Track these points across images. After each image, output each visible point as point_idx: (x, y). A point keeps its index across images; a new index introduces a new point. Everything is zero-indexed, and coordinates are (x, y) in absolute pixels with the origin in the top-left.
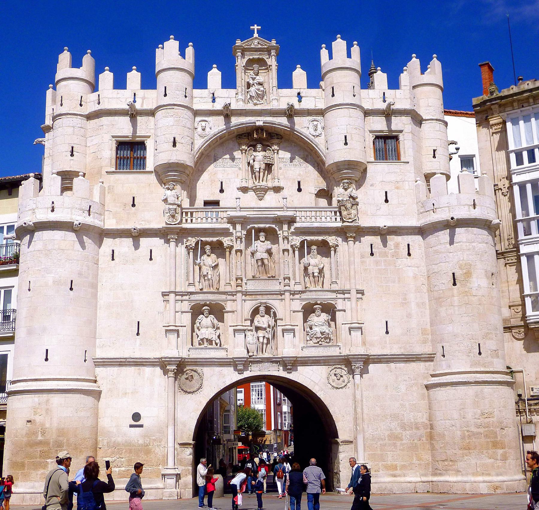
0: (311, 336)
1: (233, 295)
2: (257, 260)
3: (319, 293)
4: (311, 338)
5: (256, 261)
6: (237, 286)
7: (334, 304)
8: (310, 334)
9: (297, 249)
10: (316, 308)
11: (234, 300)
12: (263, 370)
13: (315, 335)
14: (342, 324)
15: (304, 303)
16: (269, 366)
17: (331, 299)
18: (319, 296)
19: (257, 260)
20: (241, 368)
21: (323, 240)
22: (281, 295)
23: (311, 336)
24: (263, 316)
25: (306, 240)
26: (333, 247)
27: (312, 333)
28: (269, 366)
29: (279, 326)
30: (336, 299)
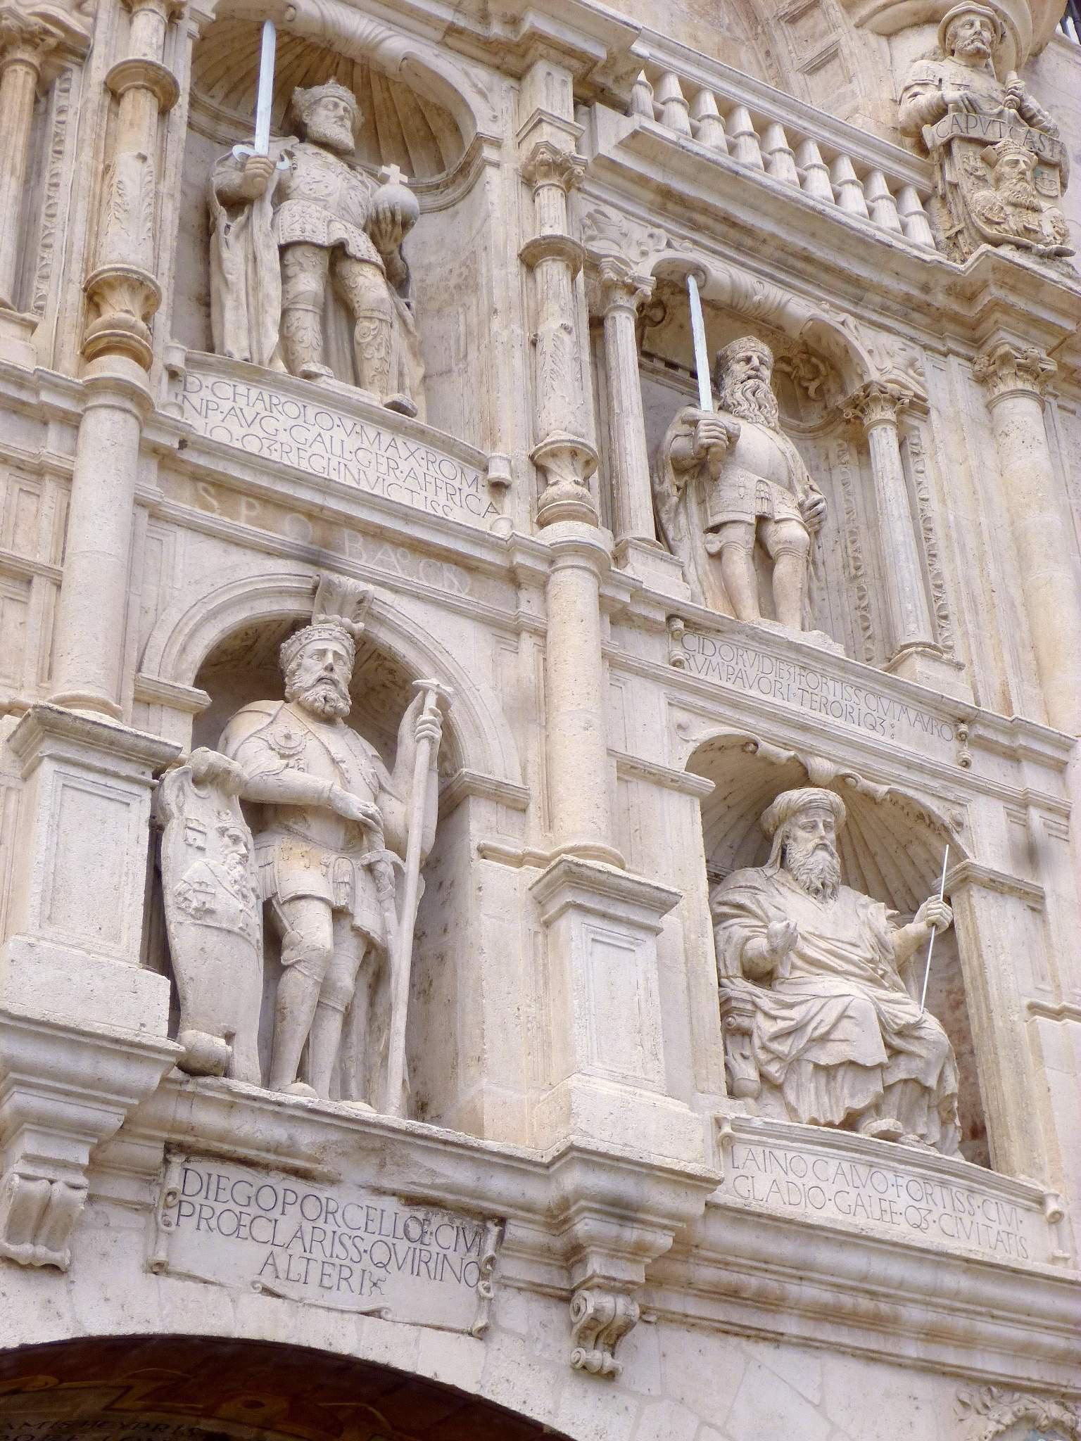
0: (782, 1047)
1: (42, 418)
2: (284, 249)
3: (833, 690)
4: (773, 1069)
5: (270, 258)
6: (91, 352)
7: (947, 820)
8: (770, 1027)
9: (633, 303)
10: (805, 808)
11: (39, 471)
12: (311, 1292)
13: (824, 1039)
14: (1034, 1008)
15: (705, 731)
16: (380, 1254)
17: (921, 768)
18: (826, 706)
19: (284, 249)
20: (58, 1189)
21: (820, 330)
22: (513, 578)
23: (782, 1047)
24: (327, 719)
25: (698, 271)
26: (895, 400)
27: (797, 1014)
28: (380, 1254)
29: (484, 852)
30: (961, 782)
